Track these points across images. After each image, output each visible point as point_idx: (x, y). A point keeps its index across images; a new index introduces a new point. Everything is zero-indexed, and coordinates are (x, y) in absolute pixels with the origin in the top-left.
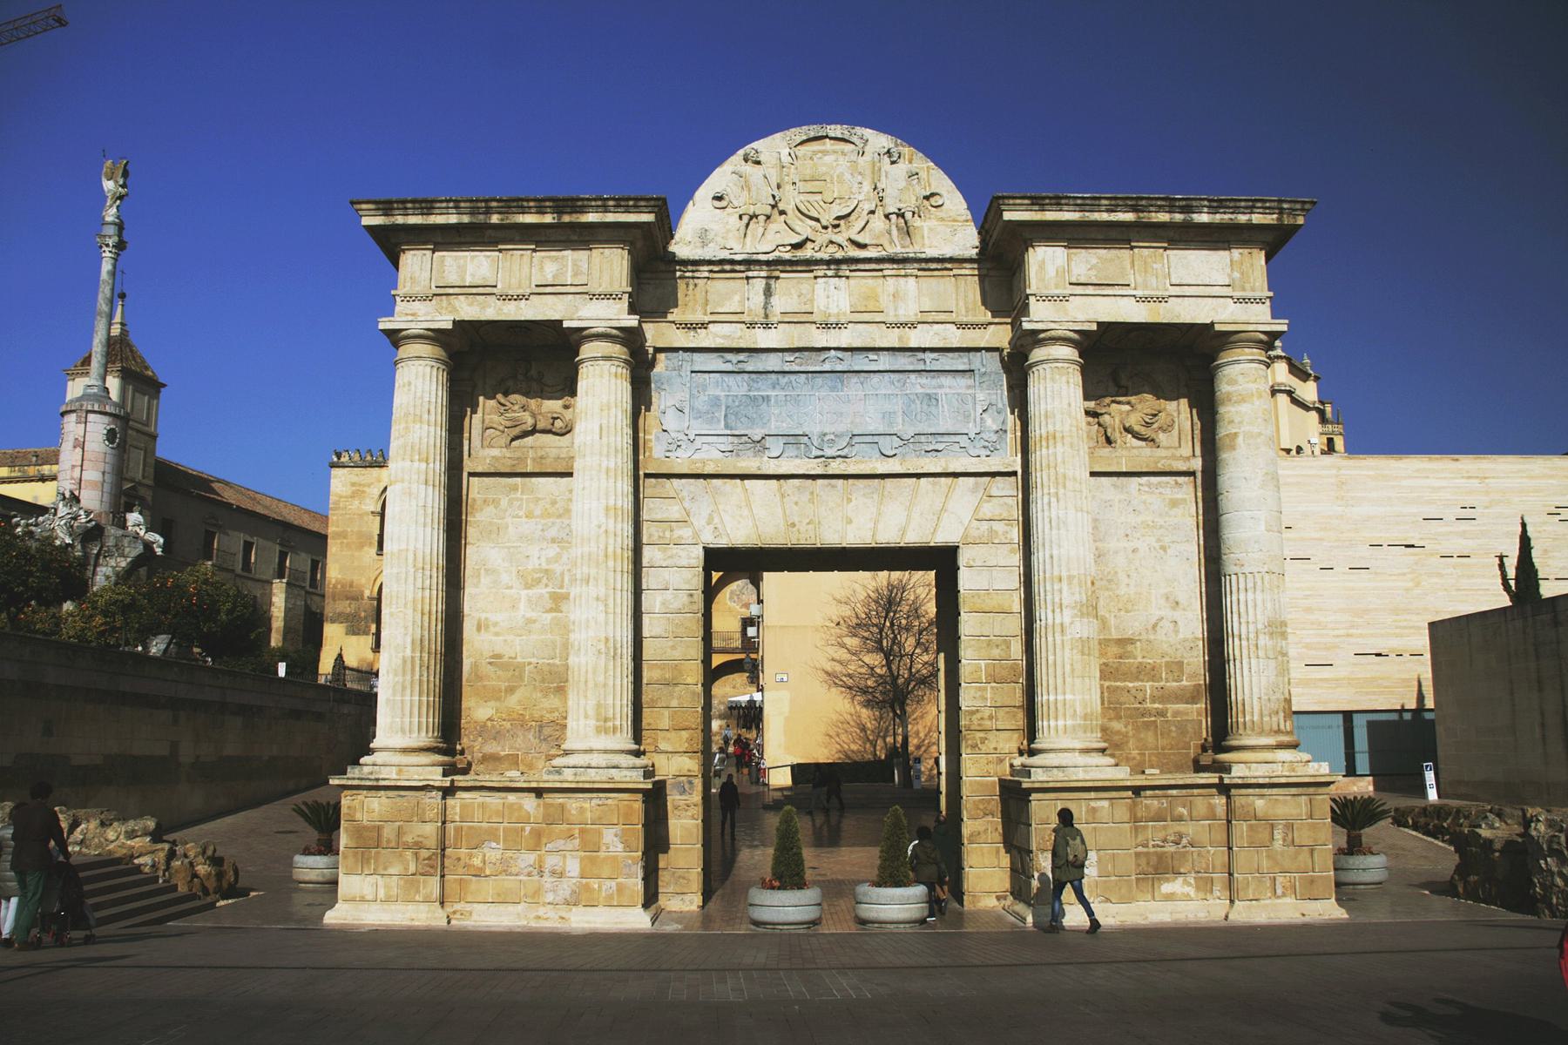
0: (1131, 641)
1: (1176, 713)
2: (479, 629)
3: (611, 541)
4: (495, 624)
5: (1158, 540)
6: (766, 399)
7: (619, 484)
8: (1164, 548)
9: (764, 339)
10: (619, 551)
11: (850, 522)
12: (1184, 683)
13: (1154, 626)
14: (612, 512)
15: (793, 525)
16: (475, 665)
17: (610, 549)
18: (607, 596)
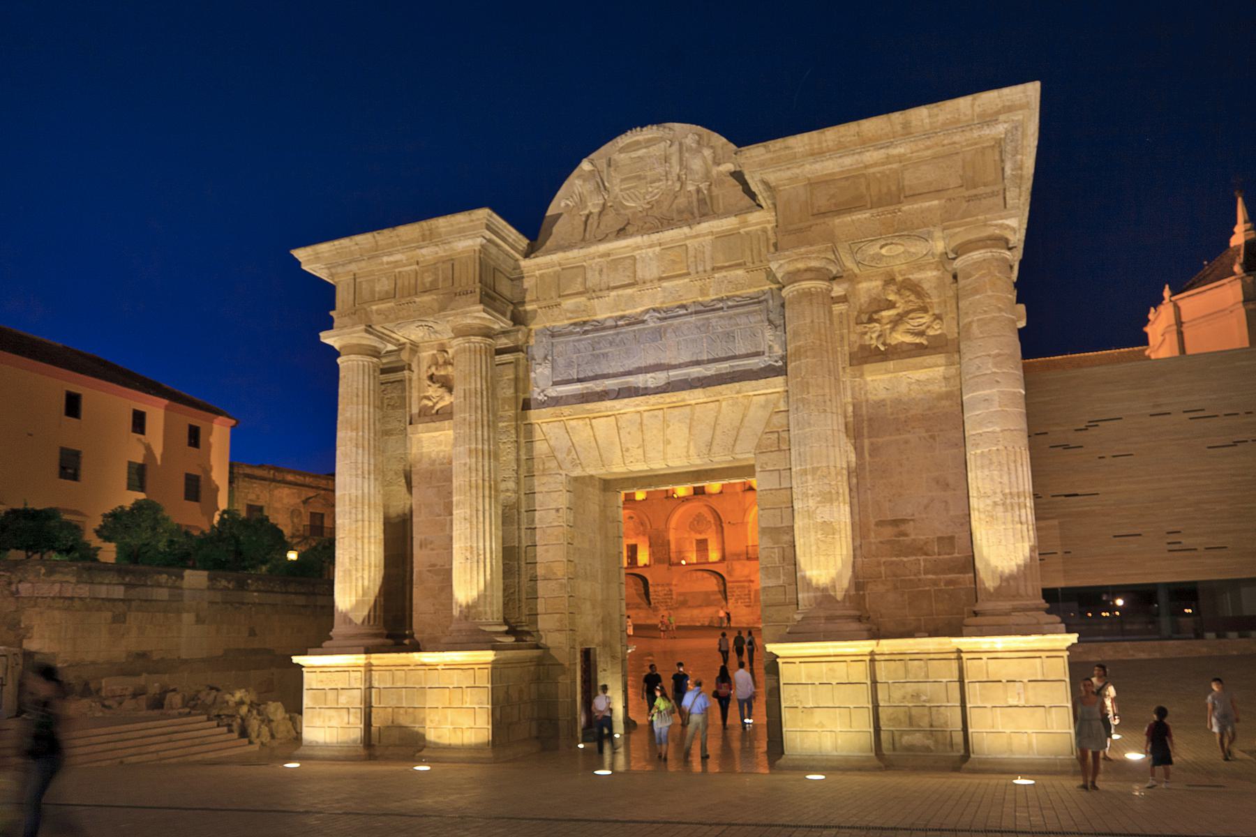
0: (904, 521)
1: (949, 582)
2: (421, 546)
3: (474, 474)
4: (431, 542)
5: (927, 431)
6: (605, 355)
7: (479, 433)
8: (933, 437)
9: (603, 310)
10: (480, 482)
11: (669, 442)
12: (956, 555)
13: (926, 507)
14: (474, 454)
15: (627, 450)
16: (420, 572)
17: (473, 482)
18: (471, 516)
